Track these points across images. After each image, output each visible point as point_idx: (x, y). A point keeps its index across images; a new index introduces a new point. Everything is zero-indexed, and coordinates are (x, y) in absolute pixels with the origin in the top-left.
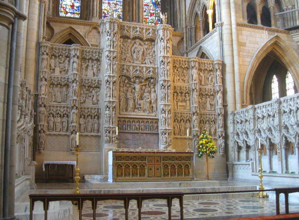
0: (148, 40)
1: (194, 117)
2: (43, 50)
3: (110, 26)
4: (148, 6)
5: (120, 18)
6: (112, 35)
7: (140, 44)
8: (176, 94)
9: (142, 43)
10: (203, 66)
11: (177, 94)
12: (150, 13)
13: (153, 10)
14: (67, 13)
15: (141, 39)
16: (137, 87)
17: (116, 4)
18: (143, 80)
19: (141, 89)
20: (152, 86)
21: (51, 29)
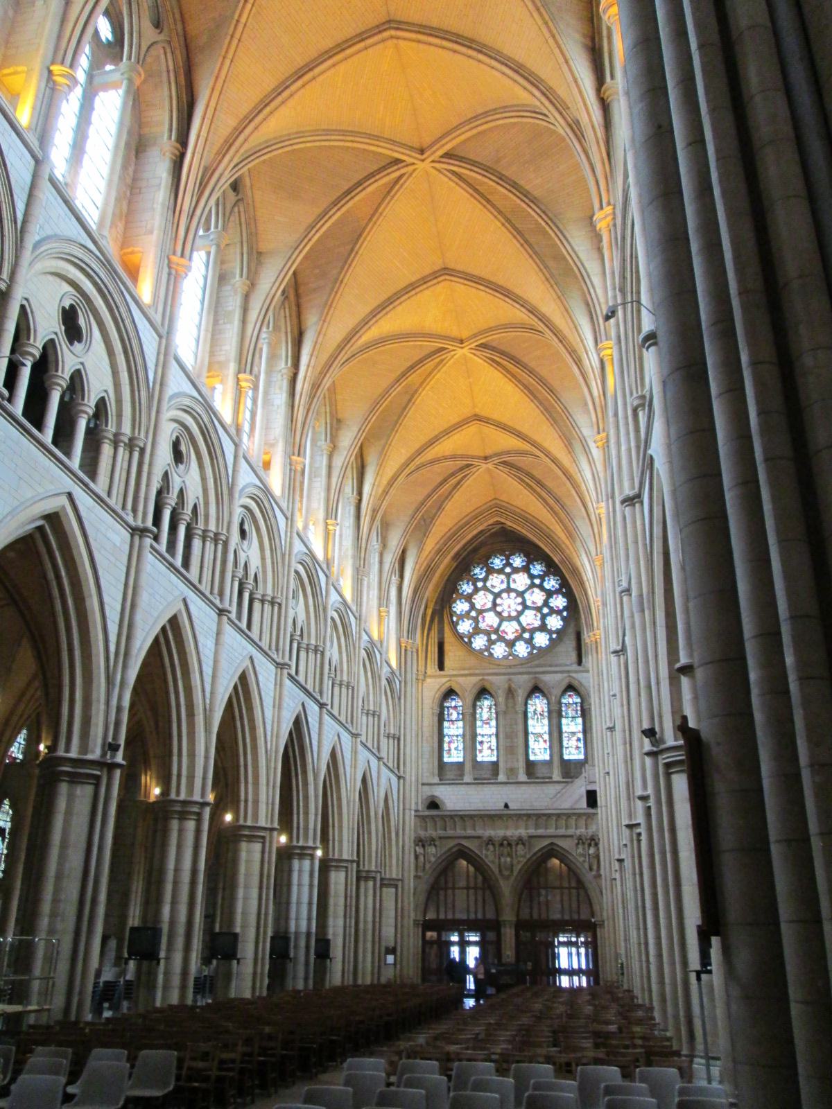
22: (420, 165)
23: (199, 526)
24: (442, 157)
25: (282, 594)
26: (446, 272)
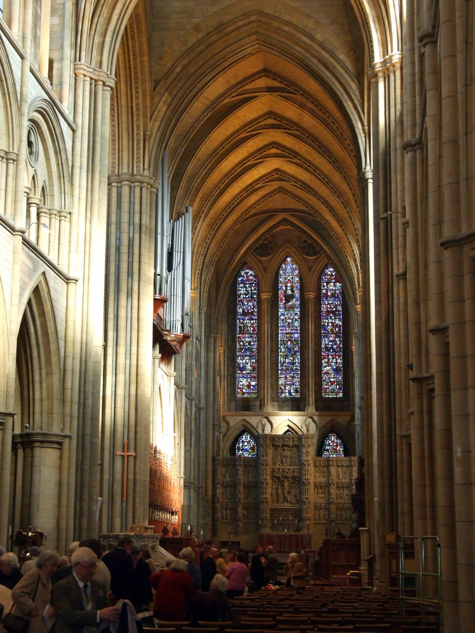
0: (294, 446)
1: (331, 506)
2: (217, 463)
3: (263, 439)
4: (328, 373)
5: (296, 391)
6: (265, 447)
7: (288, 450)
8: (316, 488)
9: (289, 449)
10: (341, 463)
11: (318, 487)
12: (330, 382)
13: (333, 378)
14: (244, 393)
15: (289, 446)
16: (286, 484)
17: (293, 377)
18: (290, 479)
19: (289, 486)
20: (297, 483)
21: (228, 423)
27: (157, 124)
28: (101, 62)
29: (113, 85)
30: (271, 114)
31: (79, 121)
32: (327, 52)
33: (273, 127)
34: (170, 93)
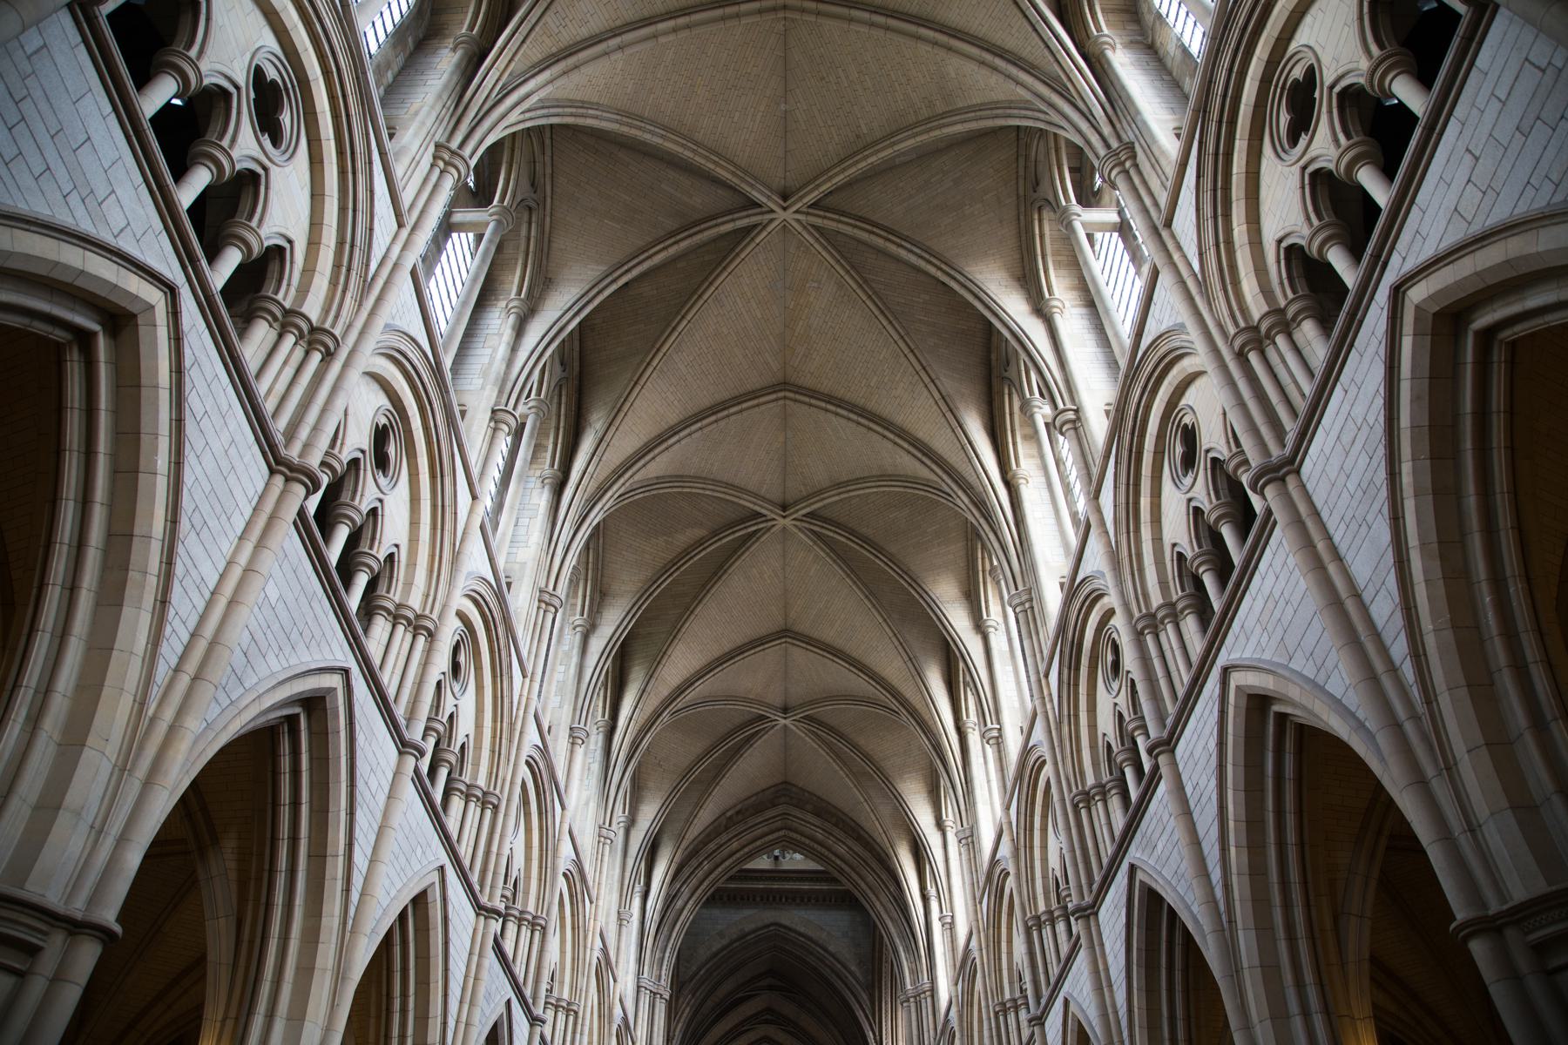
22: (781, 522)
23: (516, 906)
24: (804, 516)
25: (580, 1001)
26: (786, 633)
27: (680, 1025)
28: (660, 976)
29: (668, 998)
30: (769, 1010)
31: (639, 1033)
32: (839, 962)
33: (767, 1022)
34: (693, 996)
